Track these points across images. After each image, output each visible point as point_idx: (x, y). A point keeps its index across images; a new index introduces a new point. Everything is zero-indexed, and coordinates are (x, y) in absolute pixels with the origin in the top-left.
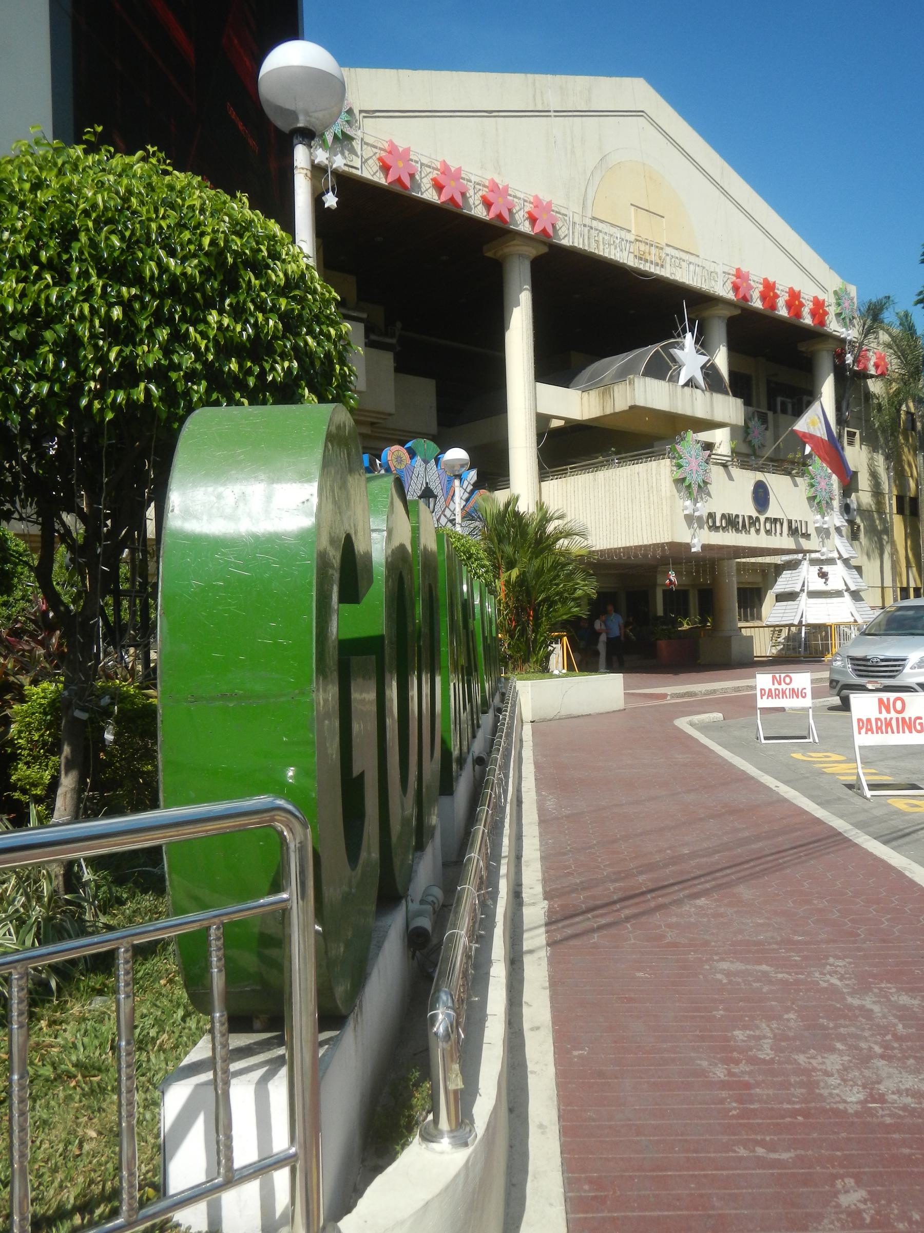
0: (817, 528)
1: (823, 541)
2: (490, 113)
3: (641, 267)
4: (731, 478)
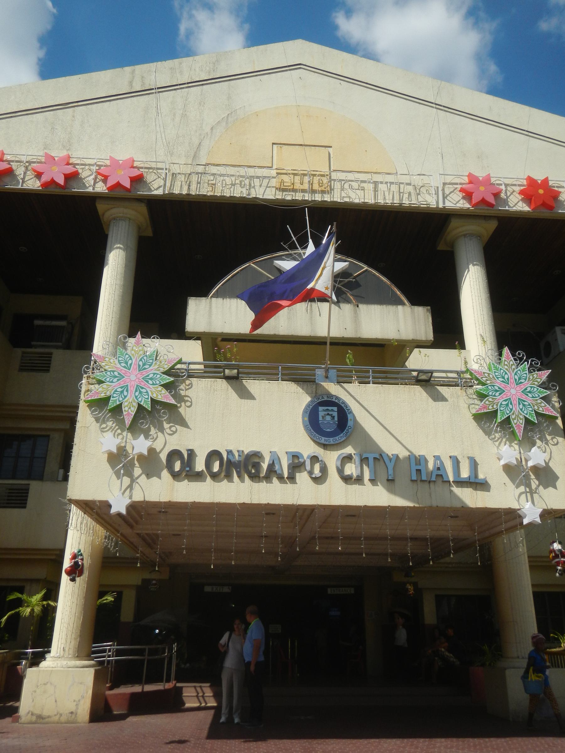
0: (509, 469)
1: (532, 492)
2: (65, 106)
3: (289, 198)
4: (250, 397)
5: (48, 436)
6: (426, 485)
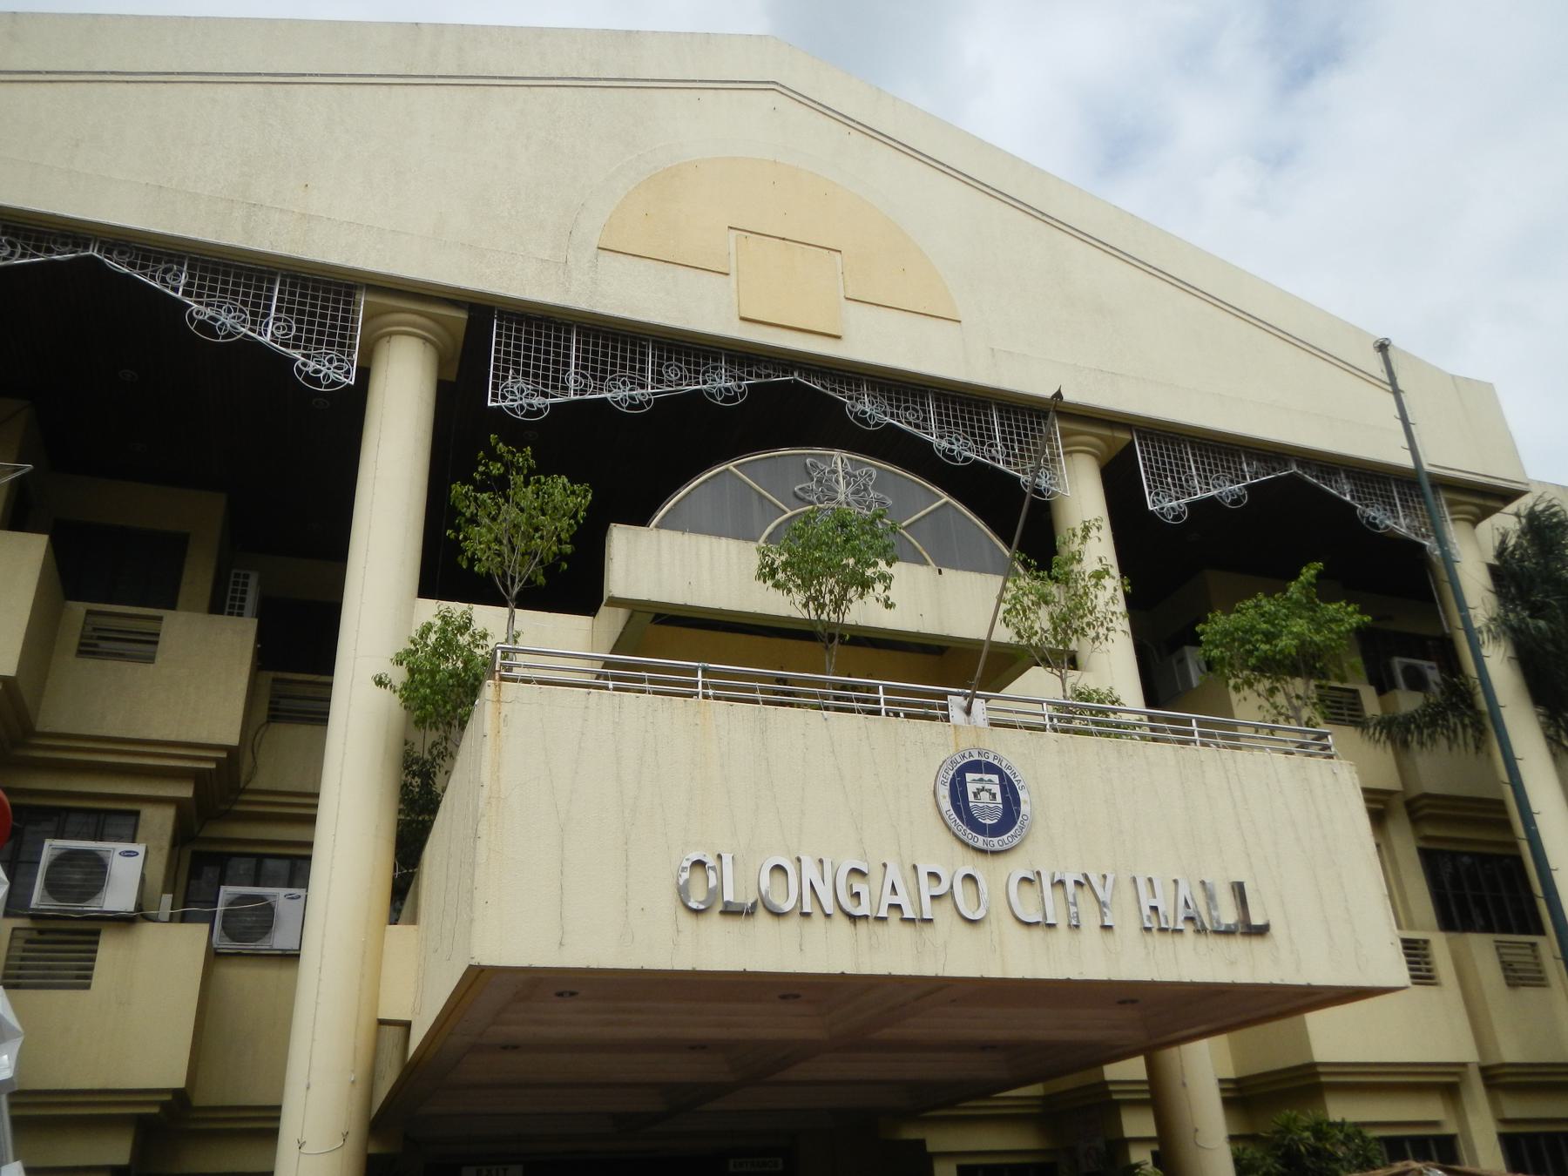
5: (137, 814)
6: (1168, 938)
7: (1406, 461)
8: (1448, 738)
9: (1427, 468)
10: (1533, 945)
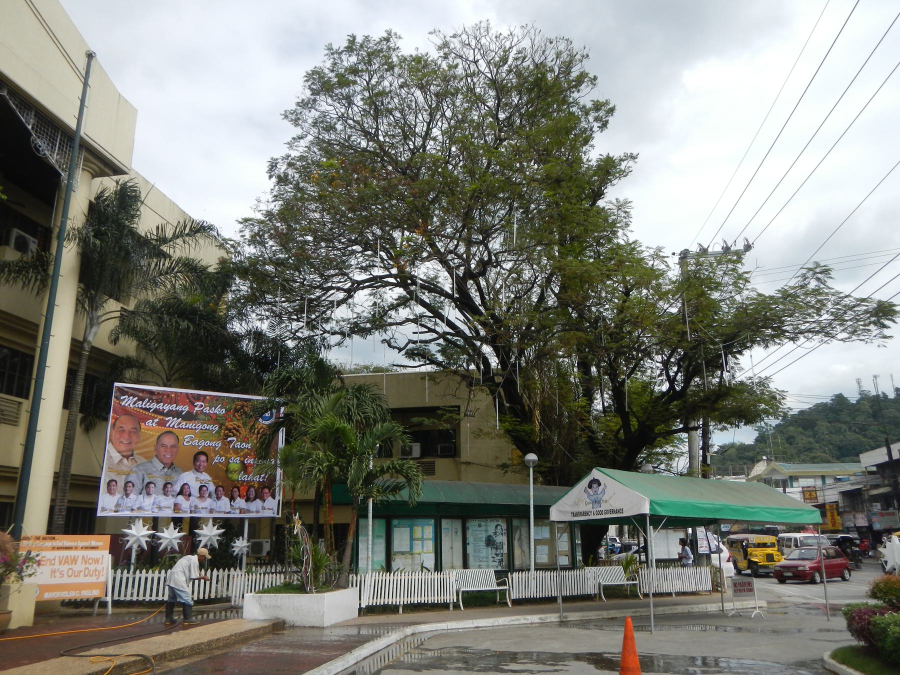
7: (73, 125)
8: (24, 283)
9: (82, 133)
10: (20, 403)
